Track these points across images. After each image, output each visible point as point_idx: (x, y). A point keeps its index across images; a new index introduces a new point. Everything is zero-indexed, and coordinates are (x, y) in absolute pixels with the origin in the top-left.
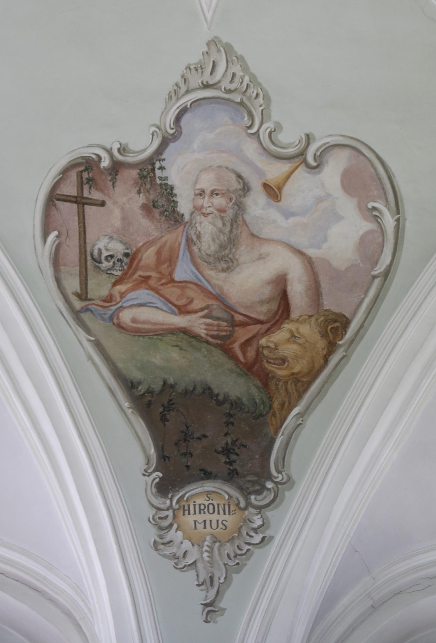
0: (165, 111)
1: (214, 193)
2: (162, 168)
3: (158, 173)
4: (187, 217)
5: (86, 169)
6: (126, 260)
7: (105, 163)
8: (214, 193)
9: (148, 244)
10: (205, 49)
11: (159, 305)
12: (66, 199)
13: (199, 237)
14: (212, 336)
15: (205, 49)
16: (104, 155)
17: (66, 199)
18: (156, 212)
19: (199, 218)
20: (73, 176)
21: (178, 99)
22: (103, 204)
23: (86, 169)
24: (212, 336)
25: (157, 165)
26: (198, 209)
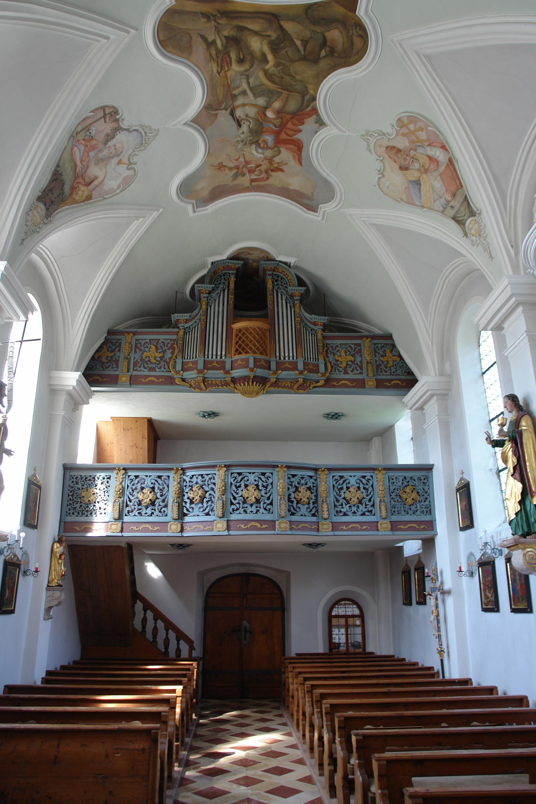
0: (136, 126)
1: (116, 149)
2: (120, 132)
3: (118, 132)
4: (107, 146)
5: (115, 112)
6: (91, 138)
7: (118, 117)
8: (116, 149)
9: (97, 141)
10: (156, 129)
11: (81, 154)
12: (104, 111)
13: (103, 152)
14: (77, 175)
15: (156, 129)
16: (120, 115)
17: (104, 111)
18: (107, 137)
19: (107, 149)
20: (112, 109)
21: (141, 128)
22: (105, 122)
23: (115, 112)
24: (77, 175)
25: (120, 131)
26: (110, 147)
